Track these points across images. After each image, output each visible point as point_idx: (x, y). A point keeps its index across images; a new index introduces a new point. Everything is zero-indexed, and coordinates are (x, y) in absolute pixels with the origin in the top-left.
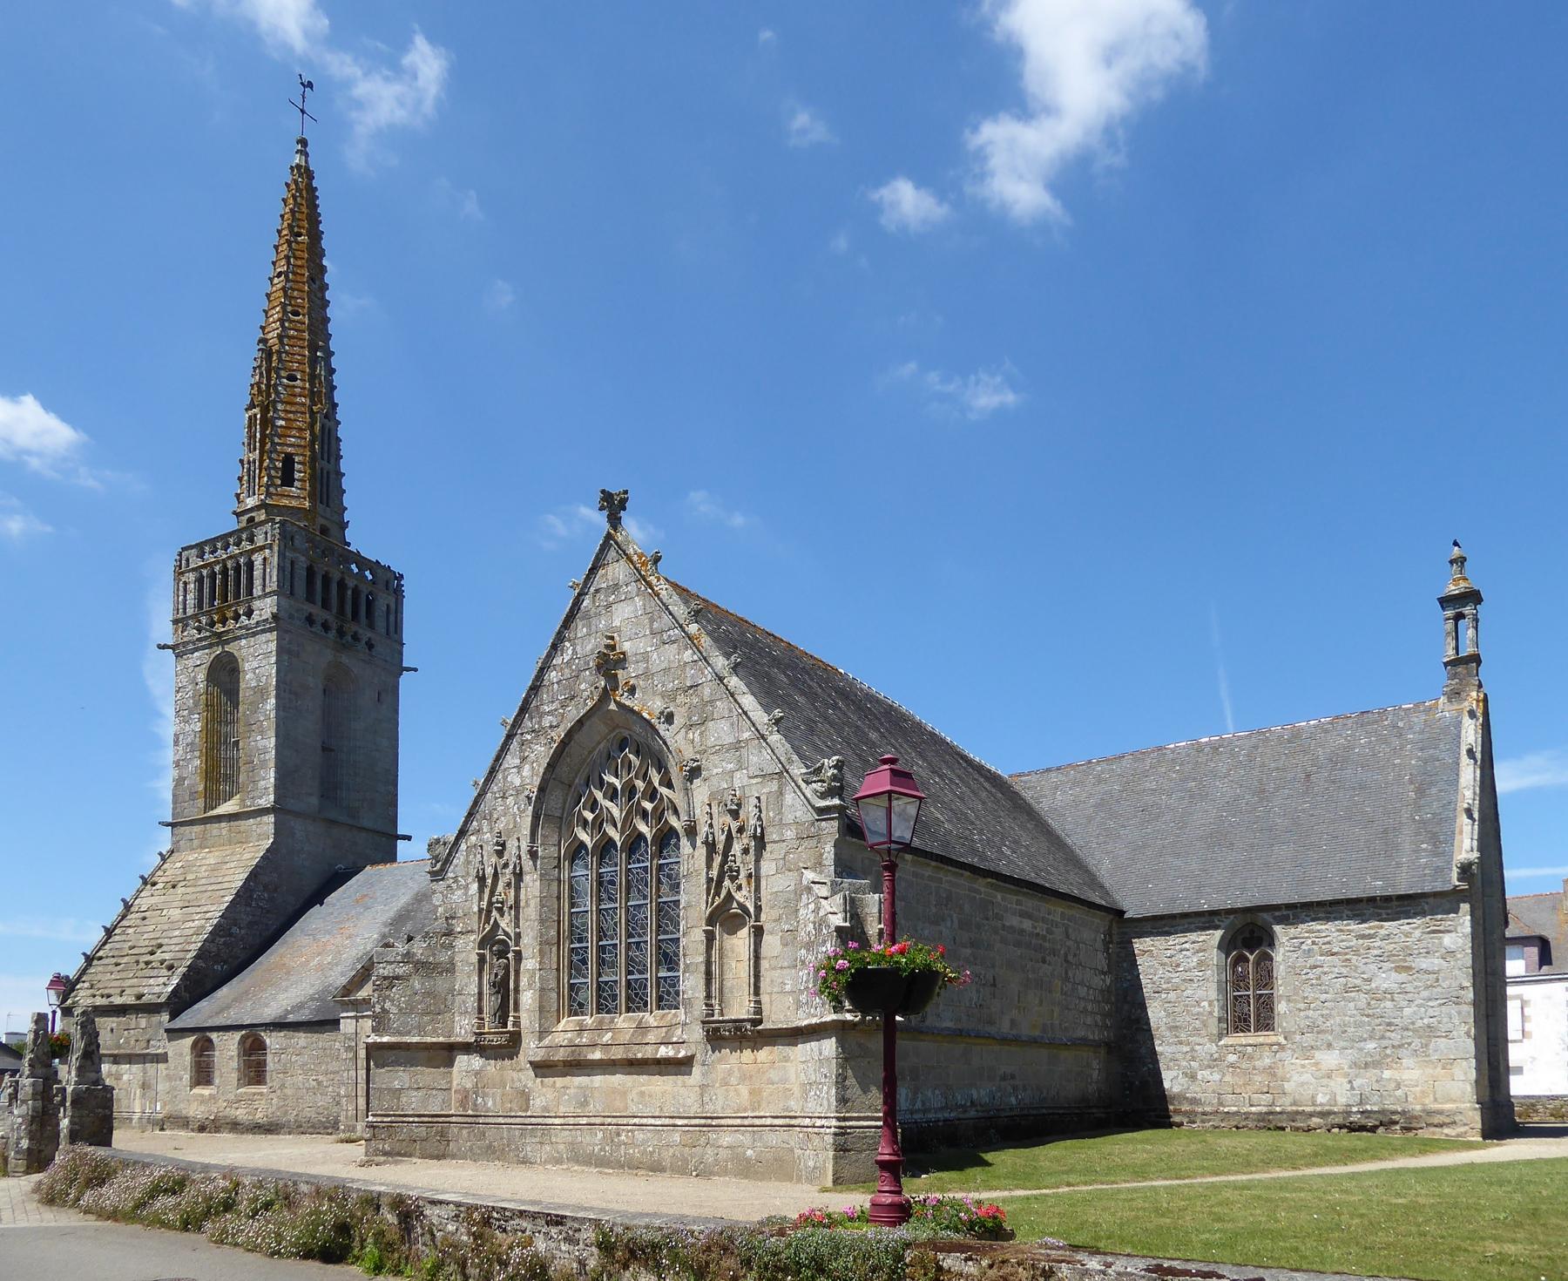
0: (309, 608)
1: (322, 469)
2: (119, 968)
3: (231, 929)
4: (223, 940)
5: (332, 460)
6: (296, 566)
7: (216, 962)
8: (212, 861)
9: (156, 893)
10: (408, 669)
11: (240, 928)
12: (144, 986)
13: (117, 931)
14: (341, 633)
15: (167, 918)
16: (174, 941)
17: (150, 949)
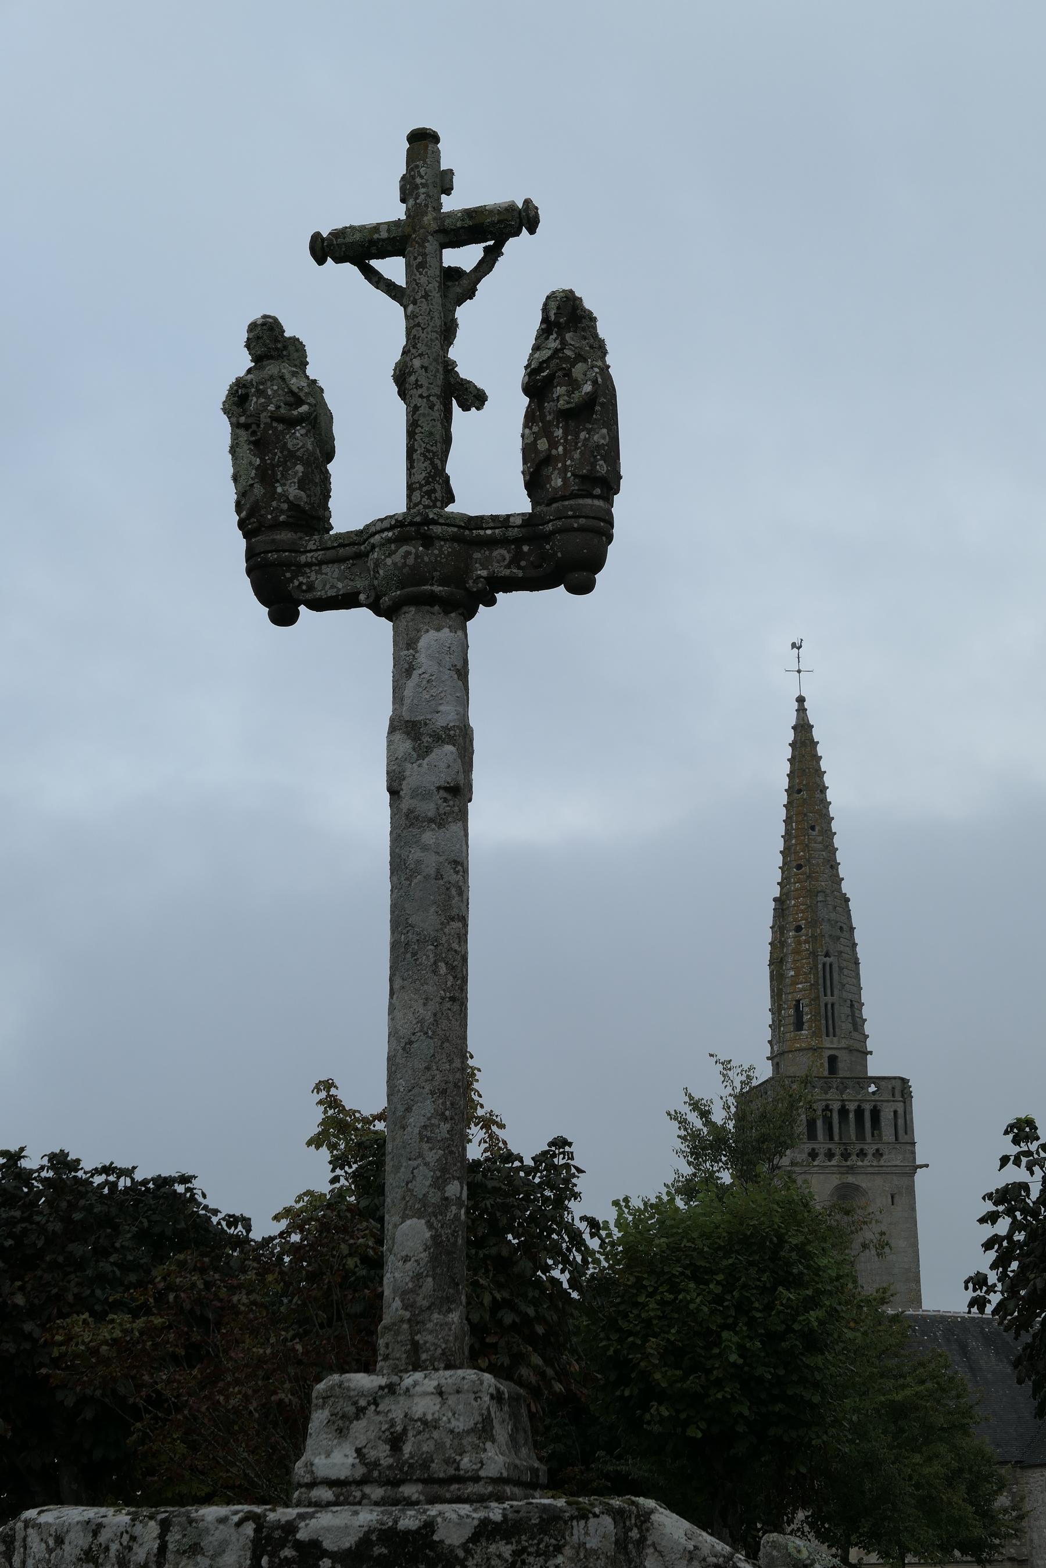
1: (826, 1005)
5: (836, 992)
10: (921, 1167)
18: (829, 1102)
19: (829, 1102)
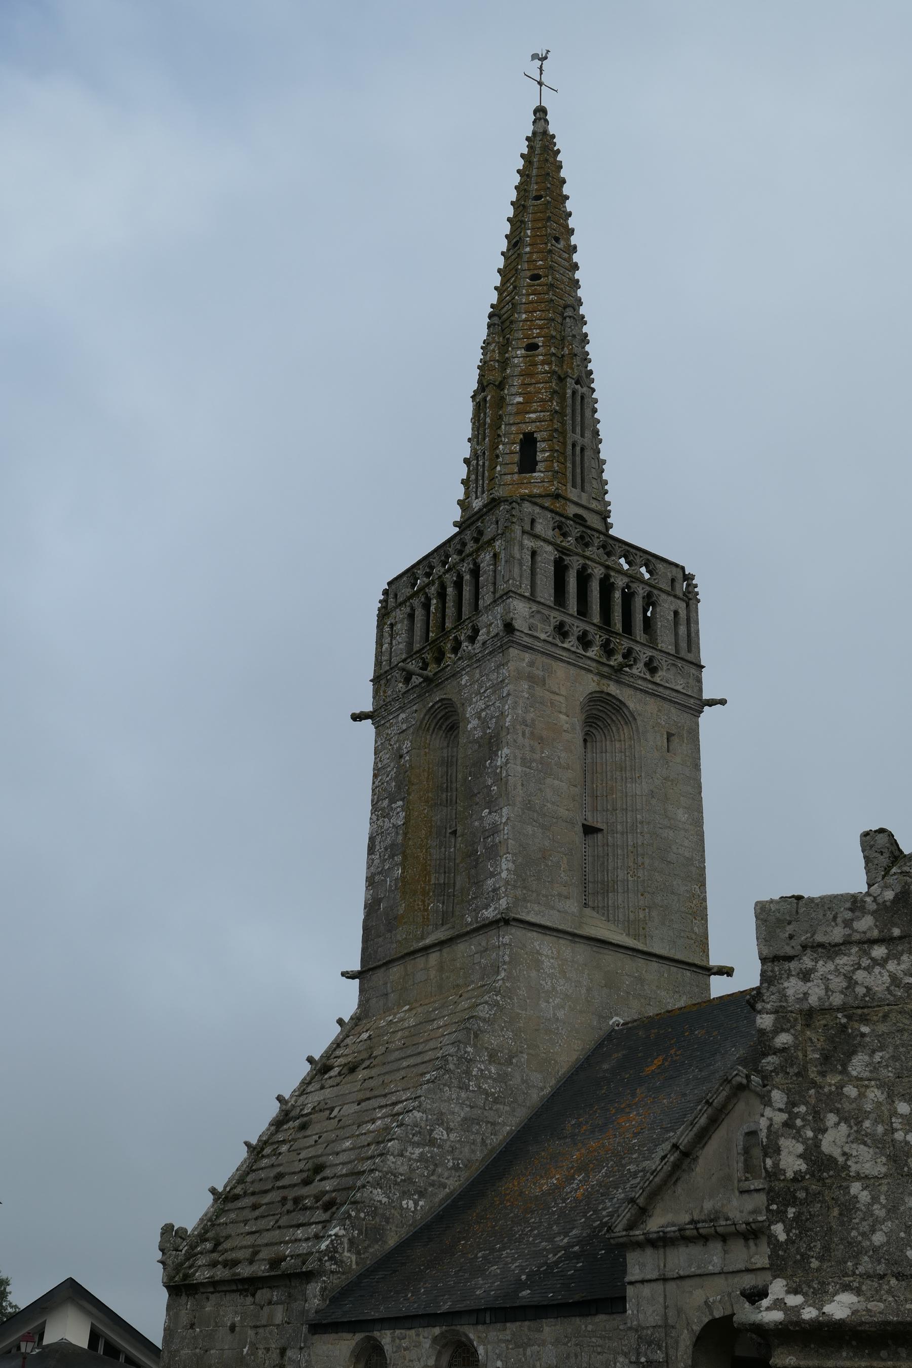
0: (556, 616)
1: (574, 446)
2: (257, 1213)
3: (432, 1131)
4: (418, 1151)
6: (539, 559)
7: (405, 1194)
8: (412, 1022)
9: (330, 1082)
11: (449, 1130)
12: (287, 1243)
13: (267, 1151)
14: (608, 650)
15: (337, 1120)
16: (343, 1157)
17: (305, 1175)
18: (587, 562)
19: (587, 562)
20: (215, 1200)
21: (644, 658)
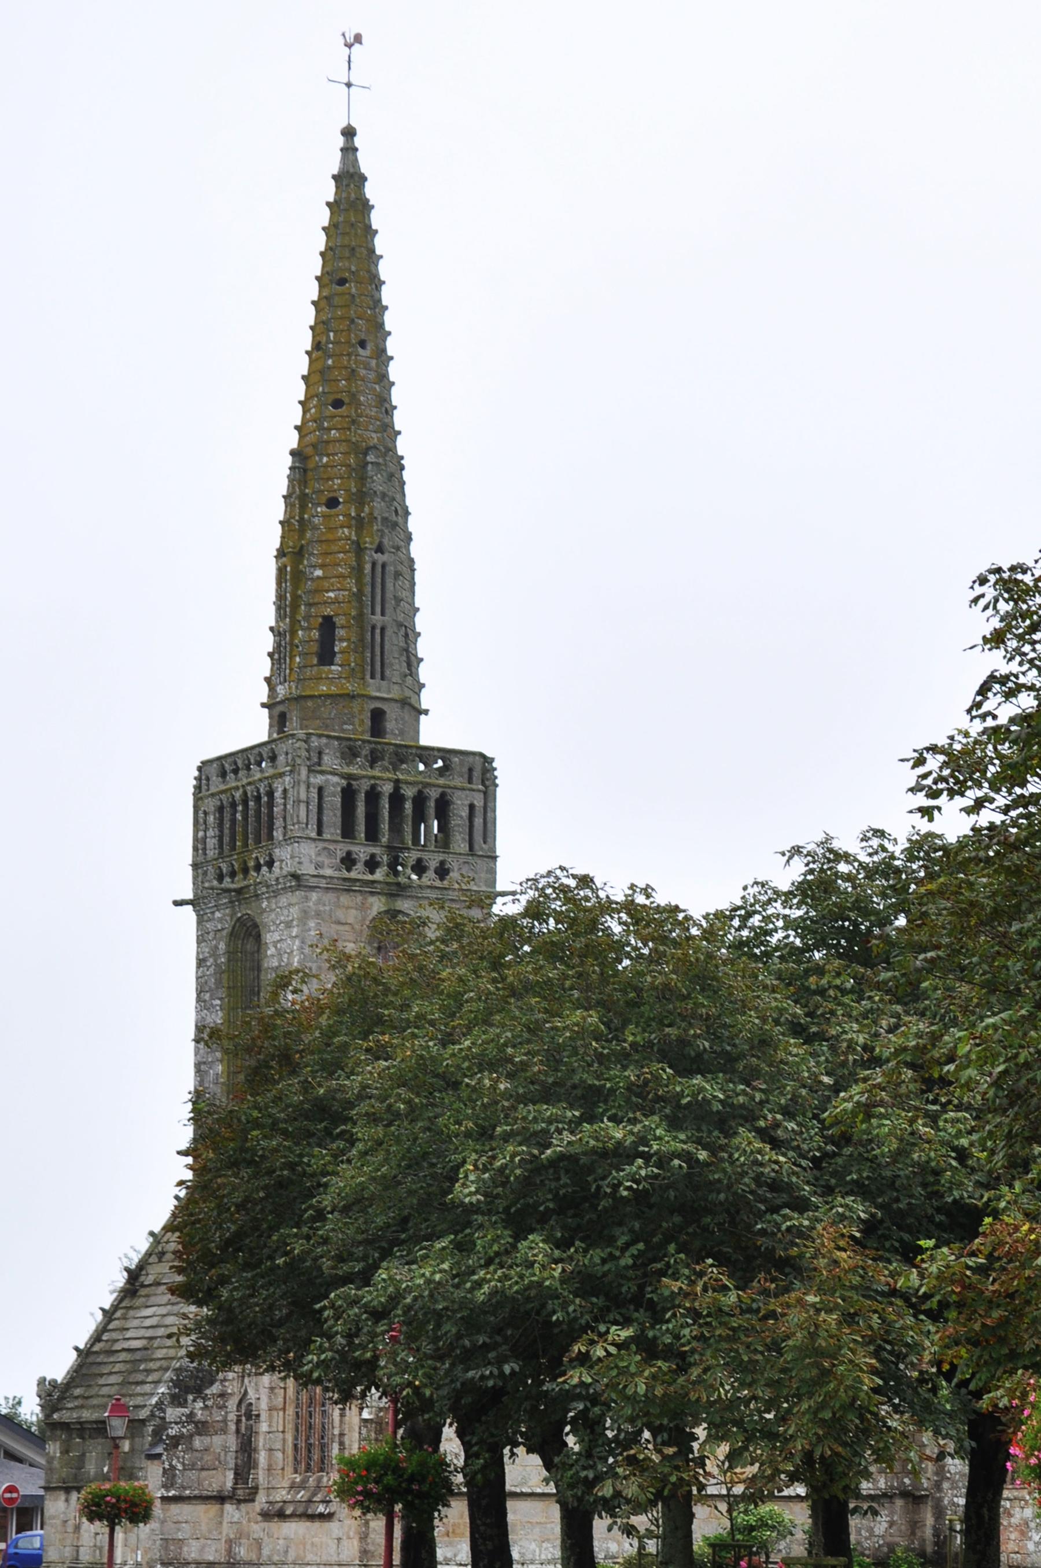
20: (79, 1356)
21: (433, 864)
